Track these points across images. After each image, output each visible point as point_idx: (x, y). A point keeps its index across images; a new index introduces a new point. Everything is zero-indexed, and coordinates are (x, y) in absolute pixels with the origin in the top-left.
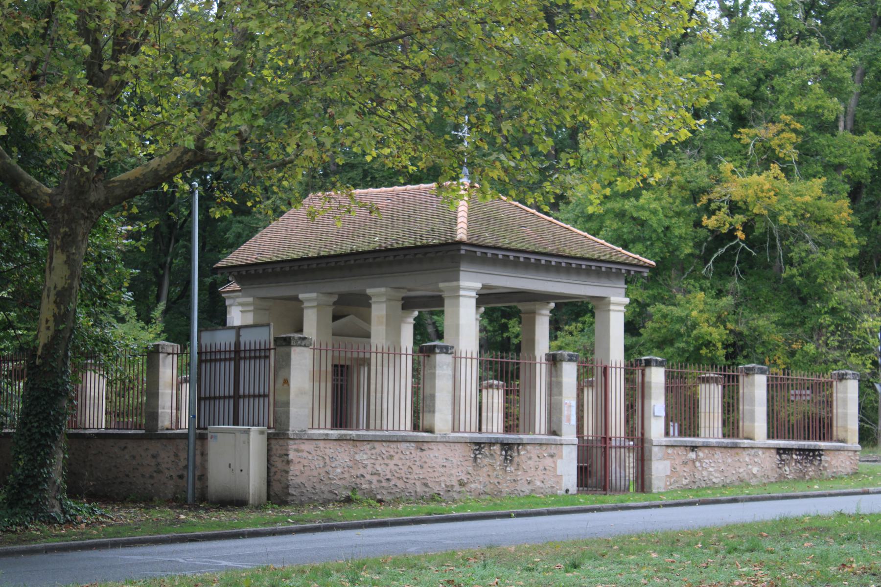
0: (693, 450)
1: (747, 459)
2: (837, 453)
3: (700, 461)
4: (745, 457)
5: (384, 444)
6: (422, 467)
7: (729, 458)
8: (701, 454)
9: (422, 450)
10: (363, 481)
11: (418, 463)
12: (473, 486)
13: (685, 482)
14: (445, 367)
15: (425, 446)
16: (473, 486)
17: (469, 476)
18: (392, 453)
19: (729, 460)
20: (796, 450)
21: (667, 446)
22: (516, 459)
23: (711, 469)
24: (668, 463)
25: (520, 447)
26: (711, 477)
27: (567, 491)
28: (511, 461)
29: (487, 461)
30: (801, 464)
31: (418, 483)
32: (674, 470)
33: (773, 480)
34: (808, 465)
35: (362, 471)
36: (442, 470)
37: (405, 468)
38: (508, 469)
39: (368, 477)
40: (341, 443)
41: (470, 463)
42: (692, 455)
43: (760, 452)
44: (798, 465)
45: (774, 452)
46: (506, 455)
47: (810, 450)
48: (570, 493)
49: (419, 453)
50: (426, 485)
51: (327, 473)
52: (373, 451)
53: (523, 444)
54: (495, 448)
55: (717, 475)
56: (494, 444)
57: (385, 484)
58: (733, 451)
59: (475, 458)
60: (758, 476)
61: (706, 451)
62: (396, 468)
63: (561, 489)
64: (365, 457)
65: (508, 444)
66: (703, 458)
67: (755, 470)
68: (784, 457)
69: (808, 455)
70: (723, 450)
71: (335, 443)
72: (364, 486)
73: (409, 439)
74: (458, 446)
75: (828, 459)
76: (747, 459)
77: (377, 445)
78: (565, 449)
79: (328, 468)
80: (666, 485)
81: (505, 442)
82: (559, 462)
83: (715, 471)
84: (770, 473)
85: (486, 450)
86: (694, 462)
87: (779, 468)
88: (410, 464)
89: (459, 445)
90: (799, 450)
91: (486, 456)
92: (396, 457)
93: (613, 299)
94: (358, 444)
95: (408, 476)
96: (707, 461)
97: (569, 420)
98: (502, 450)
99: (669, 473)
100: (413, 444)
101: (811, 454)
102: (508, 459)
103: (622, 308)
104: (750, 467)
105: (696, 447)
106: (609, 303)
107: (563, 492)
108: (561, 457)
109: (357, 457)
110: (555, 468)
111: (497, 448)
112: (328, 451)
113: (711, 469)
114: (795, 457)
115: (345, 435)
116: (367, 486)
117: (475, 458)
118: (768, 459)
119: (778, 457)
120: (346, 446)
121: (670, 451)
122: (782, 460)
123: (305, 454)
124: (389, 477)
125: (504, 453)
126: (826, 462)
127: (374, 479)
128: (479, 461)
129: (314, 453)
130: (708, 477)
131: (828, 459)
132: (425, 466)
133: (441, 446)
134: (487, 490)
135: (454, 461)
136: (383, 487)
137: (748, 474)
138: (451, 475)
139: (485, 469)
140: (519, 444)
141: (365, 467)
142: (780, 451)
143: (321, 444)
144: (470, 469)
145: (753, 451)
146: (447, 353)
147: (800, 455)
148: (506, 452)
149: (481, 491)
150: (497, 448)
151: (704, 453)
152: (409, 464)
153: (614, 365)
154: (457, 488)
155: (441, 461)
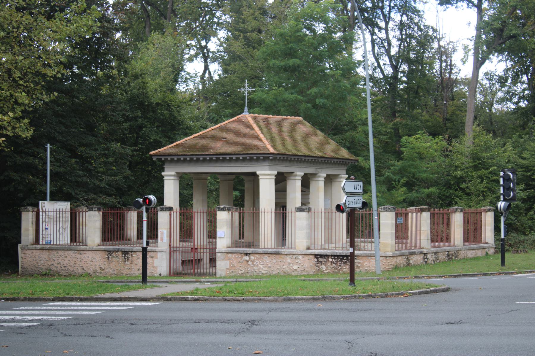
0: (246, 255)
1: (289, 261)
2: (369, 258)
3: (251, 261)
4: (288, 259)
5: (62, 251)
6: (81, 261)
7: (274, 259)
8: (252, 257)
9: (81, 254)
10: (53, 267)
11: (79, 260)
12: (107, 270)
13: (240, 272)
14: (92, 217)
15: (82, 252)
16: (107, 270)
17: (105, 266)
18: (66, 255)
19: (275, 261)
20: (332, 256)
21: (227, 253)
22: (131, 259)
23: (260, 266)
24: (228, 262)
25: (133, 253)
26: (260, 270)
27: (160, 274)
28: (128, 260)
29: (115, 259)
30: (336, 264)
31: (79, 269)
32: (232, 266)
33: (312, 273)
34: (342, 265)
35: (52, 263)
36: (91, 263)
37: (73, 262)
38: (126, 263)
39: (56, 265)
40: (43, 251)
41: (106, 260)
42: (247, 258)
43: (300, 257)
44: (333, 264)
45: (313, 257)
46: (125, 257)
47: (343, 256)
48: (162, 275)
49: (79, 255)
50: (83, 269)
51: (37, 263)
52: (58, 254)
53: (134, 252)
54: (118, 253)
55: (265, 269)
56: (118, 251)
57: (63, 268)
58: (278, 256)
59: (108, 258)
60: (299, 270)
61: (257, 256)
62: (69, 262)
63: (157, 274)
64: (54, 256)
65: (124, 251)
66: (255, 260)
67: (295, 267)
68: (321, 260)
69: (343, 259)
70: (270, 255)
71: (40, 251)
72: (53, 269)
73: (73, 249)
74: (98, 252)
75: (359, 261)
76: (289, 261)
77: (59, 251)
78: (159, 254)
79: (38, 261)
80: (226, 273)
81: (123, 250)
82: (155, 260)
83: (264, 267)
84: (309, 269)
85: (114, 254)
86: (247, 261)
87: (318, 266)
88: (75, 260)
89: (99, 252)
90: (334, 256)
91: (114, 257)
92: (69, 257)
93: (258, 173)
94: (50, 251)
95: (75, 265)
96: (257, 261)
97: (162, 240)
98: (123, 254)
99: (228, 267)
100: (76, 251)
101: (345, 258)
102: (126, 259)
103: (274, 177)
104: (291, 265)
105: (249, 254)
106: (258, 176)
107: (158, 275)
108: (157, 258)
109: (50, 256)
110: (153, 263)
111: (119, 253)
112: (37, 254)
113: (260, 266)
114: (330, 260)
115: (44, 247)
116: (55, 269)
117: (108, 258)
118: (308, 261)
119: (316, 260)
120: (45, 252)
121: (229, 255)
122: (318, 261)
123: (28, 255)
124: (65, 265)
125: (124, 255)
126: (359, 263)
127: (59, 266)
128: (110, 259)
129: (31, 255)
130: (258, 270)
131: (361, 261)
132: (82, 261)
133: (90, 252)
134: (115, 272)
135: (97, 259)
136: (62, 270)
137: (290, 269)
138: (95, 265)
139: (114, 263)
140: (132, 252)
141: (54, 261)
142: (316, 256)
143: (34, 251)
144: (106, 263)
145: (294, 256)
146: (92, 210)
147: (335, 259)
148: (125, 255)
149: (112, 273)
150: (119, 253)
151: (255, 257)
152: (75, 260)
153: (263, 211)
154: (99, 271)
155: (90, 259)
